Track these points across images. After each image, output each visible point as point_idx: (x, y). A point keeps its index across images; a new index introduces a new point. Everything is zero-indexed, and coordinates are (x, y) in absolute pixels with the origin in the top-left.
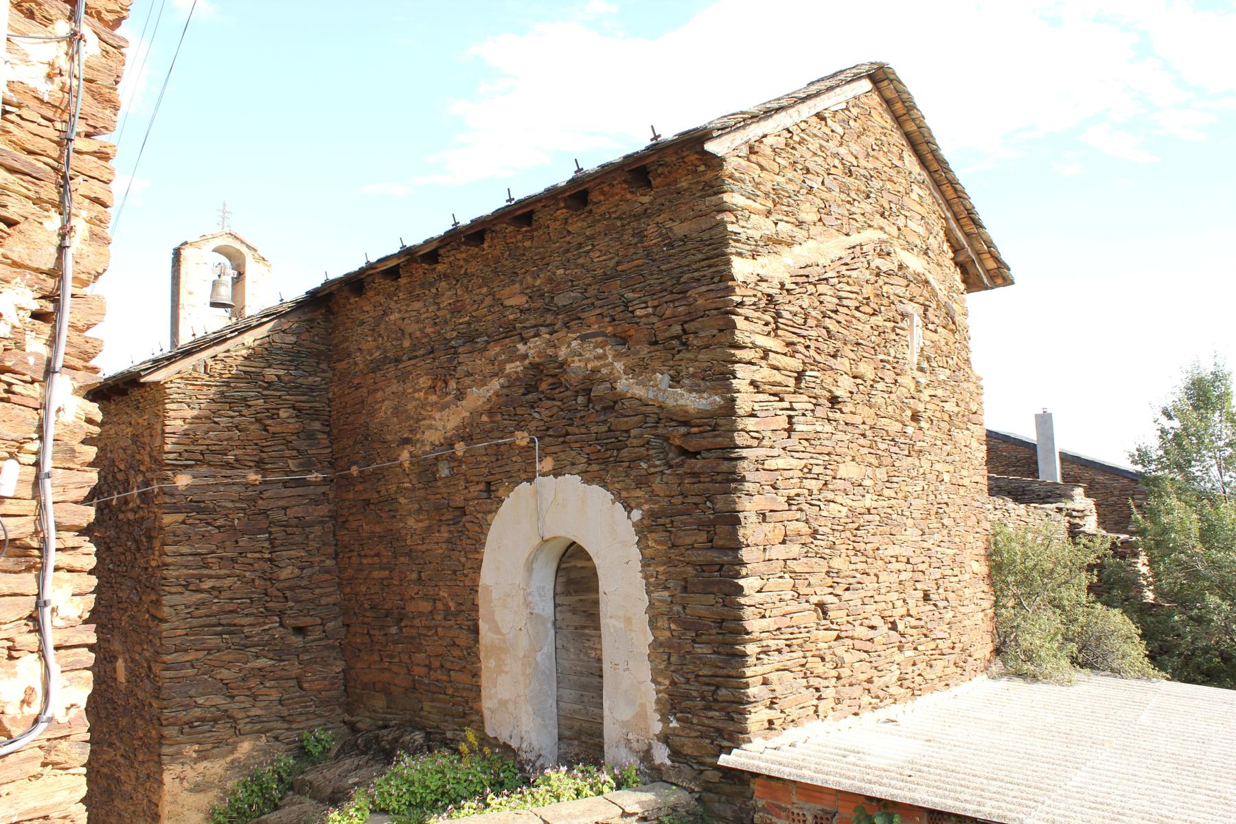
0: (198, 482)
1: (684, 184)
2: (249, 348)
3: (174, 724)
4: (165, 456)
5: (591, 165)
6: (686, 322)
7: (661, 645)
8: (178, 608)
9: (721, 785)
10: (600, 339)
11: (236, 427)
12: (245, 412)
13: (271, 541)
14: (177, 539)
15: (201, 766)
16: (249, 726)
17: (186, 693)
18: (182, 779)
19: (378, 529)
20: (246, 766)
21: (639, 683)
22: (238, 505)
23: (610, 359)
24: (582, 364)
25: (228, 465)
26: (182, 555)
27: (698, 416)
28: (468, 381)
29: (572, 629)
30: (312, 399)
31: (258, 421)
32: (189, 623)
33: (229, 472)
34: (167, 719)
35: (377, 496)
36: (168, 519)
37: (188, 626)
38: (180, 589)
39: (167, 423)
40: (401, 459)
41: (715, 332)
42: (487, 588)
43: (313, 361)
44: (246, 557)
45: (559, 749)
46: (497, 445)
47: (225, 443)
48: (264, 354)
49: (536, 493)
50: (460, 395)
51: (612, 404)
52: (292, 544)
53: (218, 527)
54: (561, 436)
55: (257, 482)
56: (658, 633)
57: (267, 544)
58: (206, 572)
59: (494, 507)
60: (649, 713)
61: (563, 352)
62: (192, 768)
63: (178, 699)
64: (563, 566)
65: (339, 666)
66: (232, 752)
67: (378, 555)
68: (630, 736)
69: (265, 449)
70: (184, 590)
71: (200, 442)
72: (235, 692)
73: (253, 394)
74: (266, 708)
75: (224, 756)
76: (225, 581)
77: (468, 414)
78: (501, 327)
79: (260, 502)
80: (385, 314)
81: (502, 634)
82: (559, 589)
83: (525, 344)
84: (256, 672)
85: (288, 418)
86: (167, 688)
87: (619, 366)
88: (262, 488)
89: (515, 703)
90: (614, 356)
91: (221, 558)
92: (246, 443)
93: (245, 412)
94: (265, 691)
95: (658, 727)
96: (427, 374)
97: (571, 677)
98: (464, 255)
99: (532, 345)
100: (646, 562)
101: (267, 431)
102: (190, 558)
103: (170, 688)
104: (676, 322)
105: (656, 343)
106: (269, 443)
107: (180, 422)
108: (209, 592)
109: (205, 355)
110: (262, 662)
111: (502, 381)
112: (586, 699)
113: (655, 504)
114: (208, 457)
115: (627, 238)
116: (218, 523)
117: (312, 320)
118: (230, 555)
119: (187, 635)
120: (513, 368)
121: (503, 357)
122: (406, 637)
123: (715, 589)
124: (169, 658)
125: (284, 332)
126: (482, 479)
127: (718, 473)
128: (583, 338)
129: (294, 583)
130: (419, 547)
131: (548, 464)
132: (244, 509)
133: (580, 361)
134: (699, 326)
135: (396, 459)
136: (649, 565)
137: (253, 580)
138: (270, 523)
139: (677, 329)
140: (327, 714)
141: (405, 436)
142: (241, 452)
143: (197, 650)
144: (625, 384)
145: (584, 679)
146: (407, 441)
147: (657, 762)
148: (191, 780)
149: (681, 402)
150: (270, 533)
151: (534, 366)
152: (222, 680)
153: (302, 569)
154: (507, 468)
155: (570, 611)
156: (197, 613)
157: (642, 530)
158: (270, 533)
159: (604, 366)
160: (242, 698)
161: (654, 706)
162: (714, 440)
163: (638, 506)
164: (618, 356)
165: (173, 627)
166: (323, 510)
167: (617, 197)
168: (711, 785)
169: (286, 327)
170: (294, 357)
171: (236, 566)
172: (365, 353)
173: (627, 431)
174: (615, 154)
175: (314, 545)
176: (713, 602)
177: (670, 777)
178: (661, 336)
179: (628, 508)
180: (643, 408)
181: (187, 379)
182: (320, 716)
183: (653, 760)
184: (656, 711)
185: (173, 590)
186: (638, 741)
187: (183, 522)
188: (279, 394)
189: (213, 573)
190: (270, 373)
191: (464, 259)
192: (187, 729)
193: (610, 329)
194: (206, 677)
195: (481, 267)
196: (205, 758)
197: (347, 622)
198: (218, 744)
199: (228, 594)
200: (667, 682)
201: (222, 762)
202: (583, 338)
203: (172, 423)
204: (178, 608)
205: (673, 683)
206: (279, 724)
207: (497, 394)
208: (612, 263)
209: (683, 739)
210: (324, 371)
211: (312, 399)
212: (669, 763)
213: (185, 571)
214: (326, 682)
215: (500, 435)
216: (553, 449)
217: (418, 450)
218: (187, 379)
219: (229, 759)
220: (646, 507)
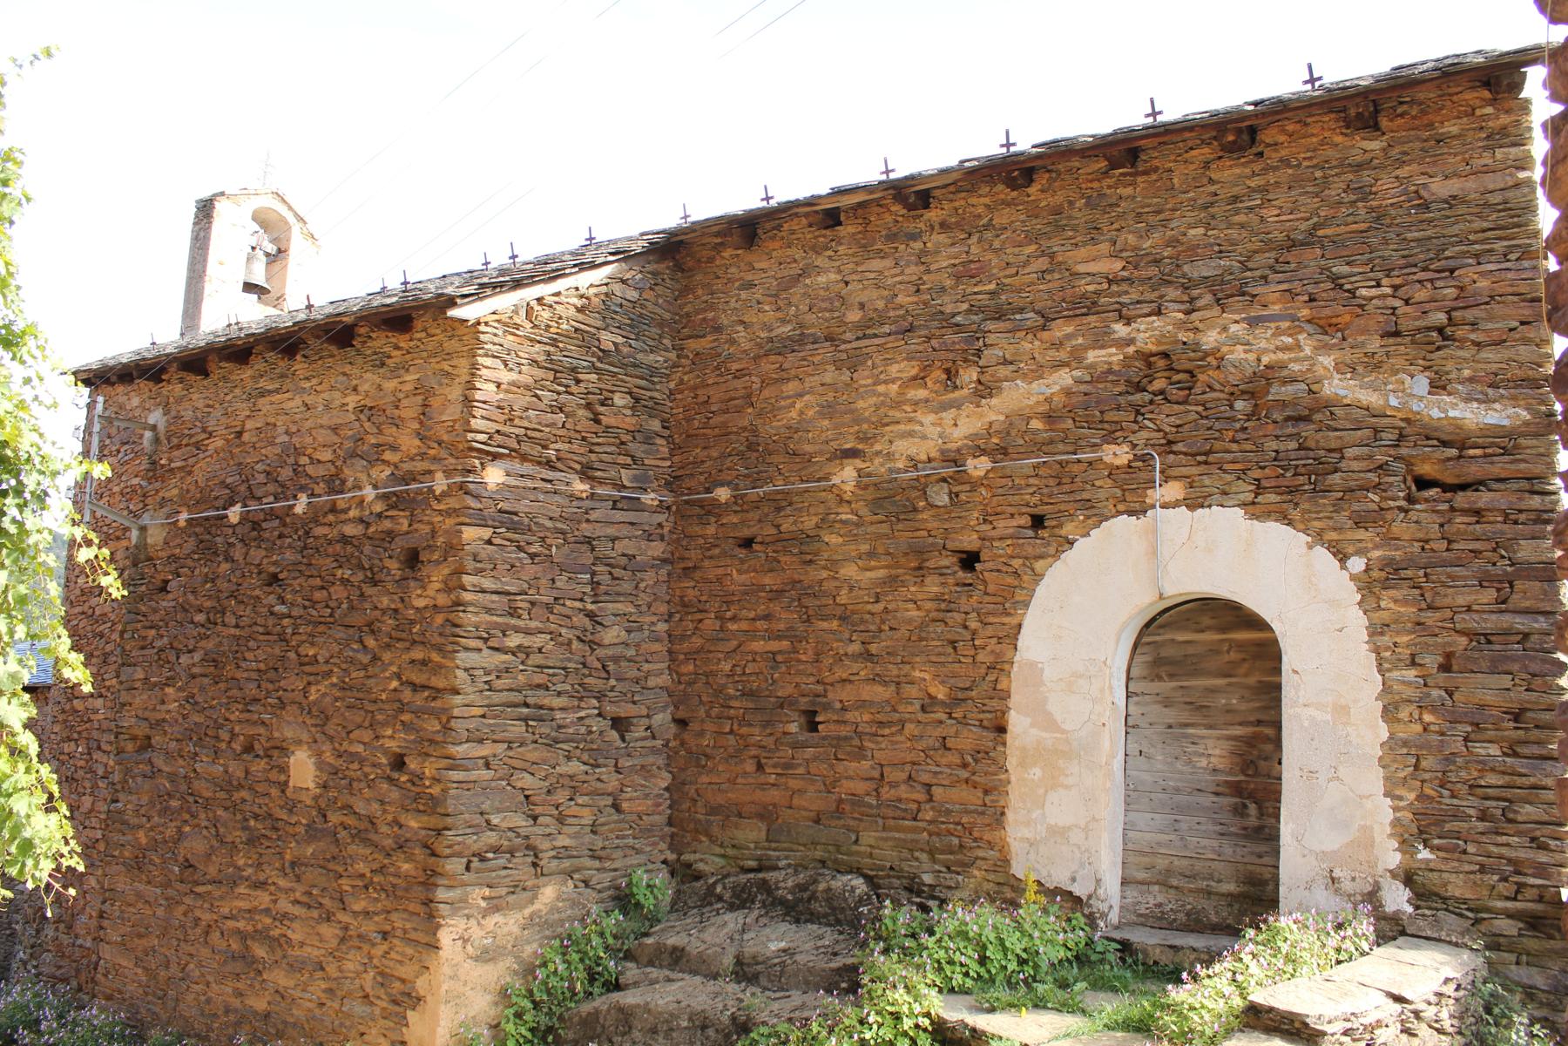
0: (512, 482)
1: (1452, 128)
2: (582, 296)
3: (459, 855)
4: (470, 436)
5: (1172, 113)
6: (1455, 309)
7: (1405, 743)
8: (476, 672)
9: (1524, 940)
10: (1285, 325)
11: (560, 409)
12: (574, 389)
13: (595, 584)
14: (478, 565)
15: (492, 921)
16: (555, 863)
17: (478, 806)
18: (466, 941)
19: (768, 580)
20: (547, 924)
21: (1361, 797)
22: (559, 525)
23: (1308, 351)
24: (1251, 357)
25: (549, 465)
26: (483, 591)
27: (1478, 434)
28: (1003, 371)
29: (1160, 729)
30: (651, 386)
31: (589, 406)
32: (488, 697)
33: (550, 475)
34: (449, 847)
35: (774, 531)
36: (470, 533)
37: (486, 702)
38: (479, 644)
39: (478, 385)
40: (836, 480)
41: (1515, 324)
42: (1033, 665)
43: (655, 331)
44: (564, 605)
45: (1123, 897)
46: (1060, 463)
47: (547, 430)
48: (604, 307)
49: (1154, 531)
50: (985, 390)
51: (1307, 412)
52: (618, 594)
53: (532, 556)
54: (1200, 454)
55: (584, 495)
56: (1398, 727)
57: (588, 589)
58: (513, 621)
59: (1052, 550)
60: (1378, 839)
61: (1210, 339)
62: (479, 924)
63: (467, 816)
64: (1146, 639)
65: (664, 780)
66: (531, 902)
67: (767, 617)
68: (1337, 873)
69: (597, 449)
70: (484, 647)
71: (517, 422)
72: (538, 810)
73: (586, 364)
74: (576, 836)
75: (521, 908)
76: (533, 638)
77: (1002, 418)
78: (1063, 300)
79: (584, 525)
80: (804, 273)
81: (1063, 732)
82: (1135, 672)
83: (1128, 324)
84: (566, 781)
85: (624, 407)
86: (453, 798)
87: (1327, 361)
88: (588, 504)
89: (1086, 830)
90: (1315, 348)
91: (533, 604)
92: (572, 434)
93: (574, 389)
94: (575, 810)
95: (1394, 859)
96: (908, 359)
97: (1153, 796)
98: (987, 200)
99: (1142, 327)
100: (1376, 631)
101: (597, 422)
102: (495, 597)
103: (457, 798)
104: (1438, 309)
105: (1397, 334)
106: (600, 440)
107: (492, 387)
108: (514, 654)
109: (530, 293)
110: (575, 767)
111: (1077, 373)
112: (1184, 826)
113: (1396, 550)
114: (526, 448)
115: (1335, 190)
116: (532, 550)
117: (655, 274)
118: (545, 599)
119: (483, 716)
120: (1110, 356)
121: (1080, 341)
122: (824, 738)
123: (1516, 667)
124: (460, 750)
125: (623, 281)
126: (1024, 510)
127: (1520, 511)
128: (1253, 322)
129: (619, 650)
130: (869, 607)
131: (1174, 490)
132: (563, 533)
133: (1246, 352)
134: (1483, 315)
135: (826, 478)
136: (1382, 634)
137: (570, 643)
138: (596, 558)
139: (1441, 318)
140: (648, 849)
141: (848, 446)
142: (566, 446)
143: (495, 741)
144: (1336, 387)
145: (1183, 799)
146: (852, 454)
147: (1390, 908)
148: (476, 944)
149: (1452, 414)
150: (593, 574)
151: (1146, 357)
152: (523, 789)
153: (629, 632)
154: (1085, 496)
155: (1159, 702)
156: (499, 684)
157: (1368, 586)
158: (593, 574)
159: (1295, 360)
160: (547, 820)
161: (1388, 830)
162: (1513, 467)
163: (1359, 553)
164: (1325, 348)
165: (467, 704)
166: (657, 549)
167: (1314, 140)
168: (1502, 940)
169: (628, 276)
170: (635, 321)
171: (552, 617)
172: (756, 327)
173: (1340, 450)
174: (1104, 124)
175: (644, 599)
176: (1509, 684)
177: (1420, 928)
178: (1405, 325)
179: (1342, 558)
180: (1373, 420)
181: (506, 324)
182: (638, 852)
183: (1381, 906)
184: (1391, 835)
185: (473, 643)
186: (1353, 879)
187: (489, 542)
188: (615, 370)
189: (521, 623)
190: (608, 339)
191: (986, 206)
192: (476, 863)
193: (1305, 312)
194: (504, 783)
195: (1023, 217)
196: (497, 909)
197: (681, 714)
198: (515, 888)
199: (536, 659)
200: (1412, 796)
201: (519, 916)
202: (1253, 322)
203: (485, 386)
204: (476, 672)
205: (1421, 797)
206: (588, 862)
207: (1068, 392)
208: (1304, 226)
209: (1445, 875)
210: (666, 350)
211: (651, 386)
212: (1410, 909)
213: (488, 618)
214: (650, 802)
215: (1070, 449)
216: (1185, 471)
217: (878, 466)
218: (506, 324)
219: (527, 912)
220: (1376, 554)
